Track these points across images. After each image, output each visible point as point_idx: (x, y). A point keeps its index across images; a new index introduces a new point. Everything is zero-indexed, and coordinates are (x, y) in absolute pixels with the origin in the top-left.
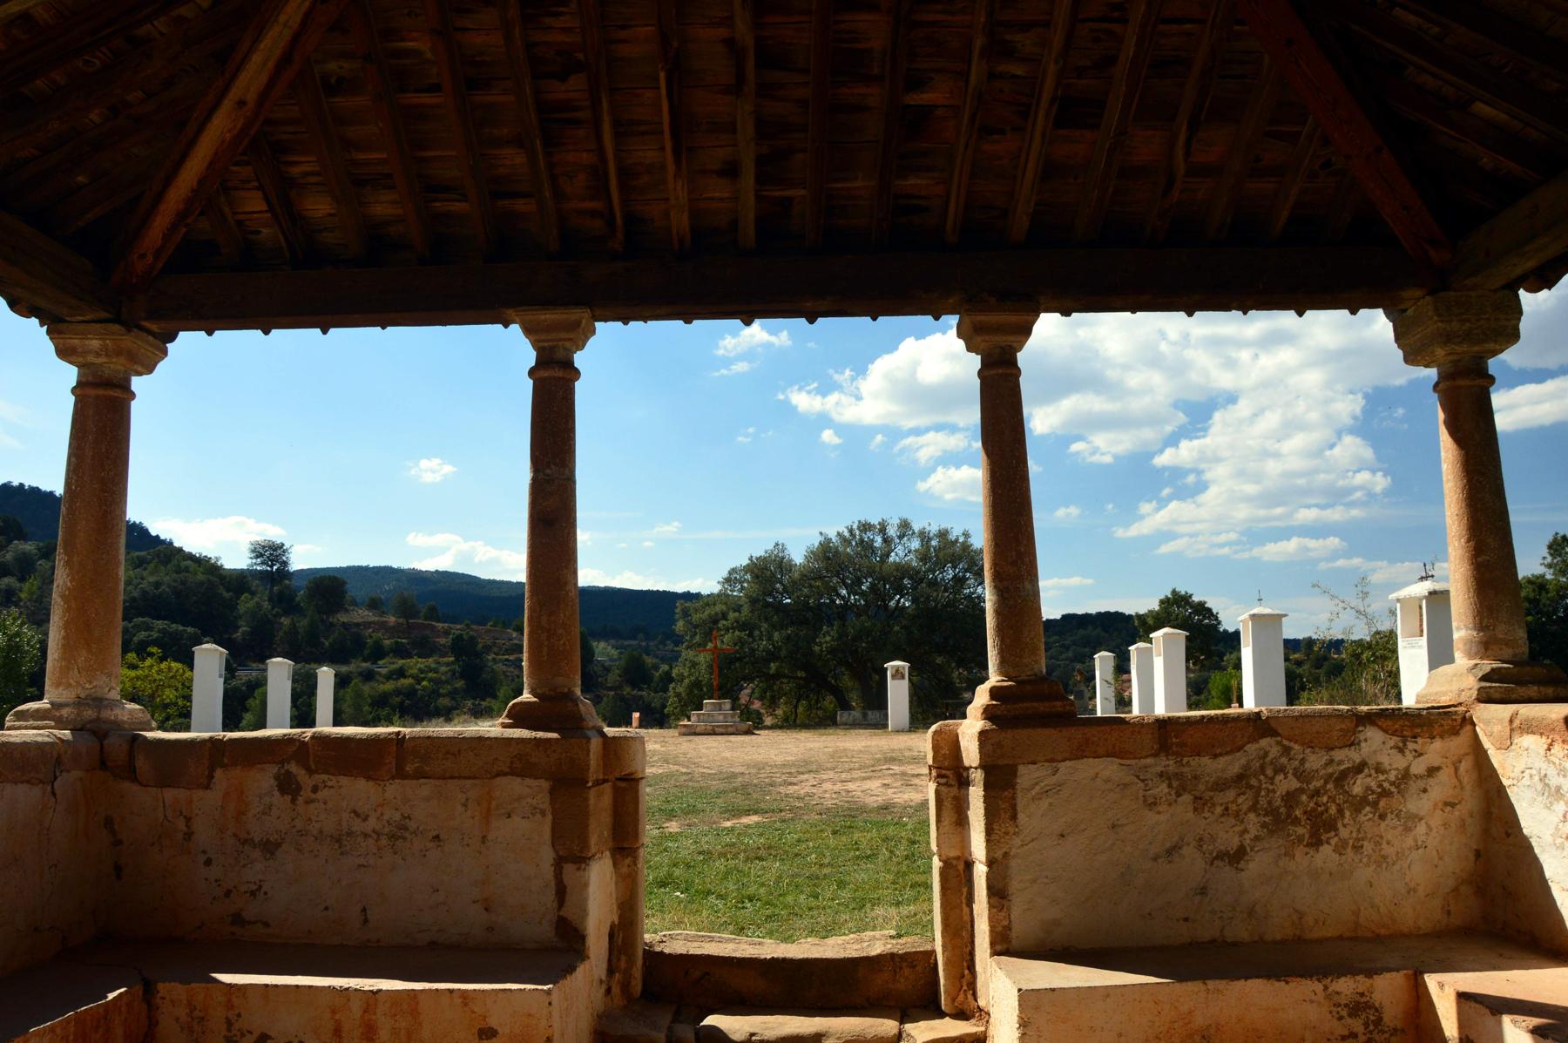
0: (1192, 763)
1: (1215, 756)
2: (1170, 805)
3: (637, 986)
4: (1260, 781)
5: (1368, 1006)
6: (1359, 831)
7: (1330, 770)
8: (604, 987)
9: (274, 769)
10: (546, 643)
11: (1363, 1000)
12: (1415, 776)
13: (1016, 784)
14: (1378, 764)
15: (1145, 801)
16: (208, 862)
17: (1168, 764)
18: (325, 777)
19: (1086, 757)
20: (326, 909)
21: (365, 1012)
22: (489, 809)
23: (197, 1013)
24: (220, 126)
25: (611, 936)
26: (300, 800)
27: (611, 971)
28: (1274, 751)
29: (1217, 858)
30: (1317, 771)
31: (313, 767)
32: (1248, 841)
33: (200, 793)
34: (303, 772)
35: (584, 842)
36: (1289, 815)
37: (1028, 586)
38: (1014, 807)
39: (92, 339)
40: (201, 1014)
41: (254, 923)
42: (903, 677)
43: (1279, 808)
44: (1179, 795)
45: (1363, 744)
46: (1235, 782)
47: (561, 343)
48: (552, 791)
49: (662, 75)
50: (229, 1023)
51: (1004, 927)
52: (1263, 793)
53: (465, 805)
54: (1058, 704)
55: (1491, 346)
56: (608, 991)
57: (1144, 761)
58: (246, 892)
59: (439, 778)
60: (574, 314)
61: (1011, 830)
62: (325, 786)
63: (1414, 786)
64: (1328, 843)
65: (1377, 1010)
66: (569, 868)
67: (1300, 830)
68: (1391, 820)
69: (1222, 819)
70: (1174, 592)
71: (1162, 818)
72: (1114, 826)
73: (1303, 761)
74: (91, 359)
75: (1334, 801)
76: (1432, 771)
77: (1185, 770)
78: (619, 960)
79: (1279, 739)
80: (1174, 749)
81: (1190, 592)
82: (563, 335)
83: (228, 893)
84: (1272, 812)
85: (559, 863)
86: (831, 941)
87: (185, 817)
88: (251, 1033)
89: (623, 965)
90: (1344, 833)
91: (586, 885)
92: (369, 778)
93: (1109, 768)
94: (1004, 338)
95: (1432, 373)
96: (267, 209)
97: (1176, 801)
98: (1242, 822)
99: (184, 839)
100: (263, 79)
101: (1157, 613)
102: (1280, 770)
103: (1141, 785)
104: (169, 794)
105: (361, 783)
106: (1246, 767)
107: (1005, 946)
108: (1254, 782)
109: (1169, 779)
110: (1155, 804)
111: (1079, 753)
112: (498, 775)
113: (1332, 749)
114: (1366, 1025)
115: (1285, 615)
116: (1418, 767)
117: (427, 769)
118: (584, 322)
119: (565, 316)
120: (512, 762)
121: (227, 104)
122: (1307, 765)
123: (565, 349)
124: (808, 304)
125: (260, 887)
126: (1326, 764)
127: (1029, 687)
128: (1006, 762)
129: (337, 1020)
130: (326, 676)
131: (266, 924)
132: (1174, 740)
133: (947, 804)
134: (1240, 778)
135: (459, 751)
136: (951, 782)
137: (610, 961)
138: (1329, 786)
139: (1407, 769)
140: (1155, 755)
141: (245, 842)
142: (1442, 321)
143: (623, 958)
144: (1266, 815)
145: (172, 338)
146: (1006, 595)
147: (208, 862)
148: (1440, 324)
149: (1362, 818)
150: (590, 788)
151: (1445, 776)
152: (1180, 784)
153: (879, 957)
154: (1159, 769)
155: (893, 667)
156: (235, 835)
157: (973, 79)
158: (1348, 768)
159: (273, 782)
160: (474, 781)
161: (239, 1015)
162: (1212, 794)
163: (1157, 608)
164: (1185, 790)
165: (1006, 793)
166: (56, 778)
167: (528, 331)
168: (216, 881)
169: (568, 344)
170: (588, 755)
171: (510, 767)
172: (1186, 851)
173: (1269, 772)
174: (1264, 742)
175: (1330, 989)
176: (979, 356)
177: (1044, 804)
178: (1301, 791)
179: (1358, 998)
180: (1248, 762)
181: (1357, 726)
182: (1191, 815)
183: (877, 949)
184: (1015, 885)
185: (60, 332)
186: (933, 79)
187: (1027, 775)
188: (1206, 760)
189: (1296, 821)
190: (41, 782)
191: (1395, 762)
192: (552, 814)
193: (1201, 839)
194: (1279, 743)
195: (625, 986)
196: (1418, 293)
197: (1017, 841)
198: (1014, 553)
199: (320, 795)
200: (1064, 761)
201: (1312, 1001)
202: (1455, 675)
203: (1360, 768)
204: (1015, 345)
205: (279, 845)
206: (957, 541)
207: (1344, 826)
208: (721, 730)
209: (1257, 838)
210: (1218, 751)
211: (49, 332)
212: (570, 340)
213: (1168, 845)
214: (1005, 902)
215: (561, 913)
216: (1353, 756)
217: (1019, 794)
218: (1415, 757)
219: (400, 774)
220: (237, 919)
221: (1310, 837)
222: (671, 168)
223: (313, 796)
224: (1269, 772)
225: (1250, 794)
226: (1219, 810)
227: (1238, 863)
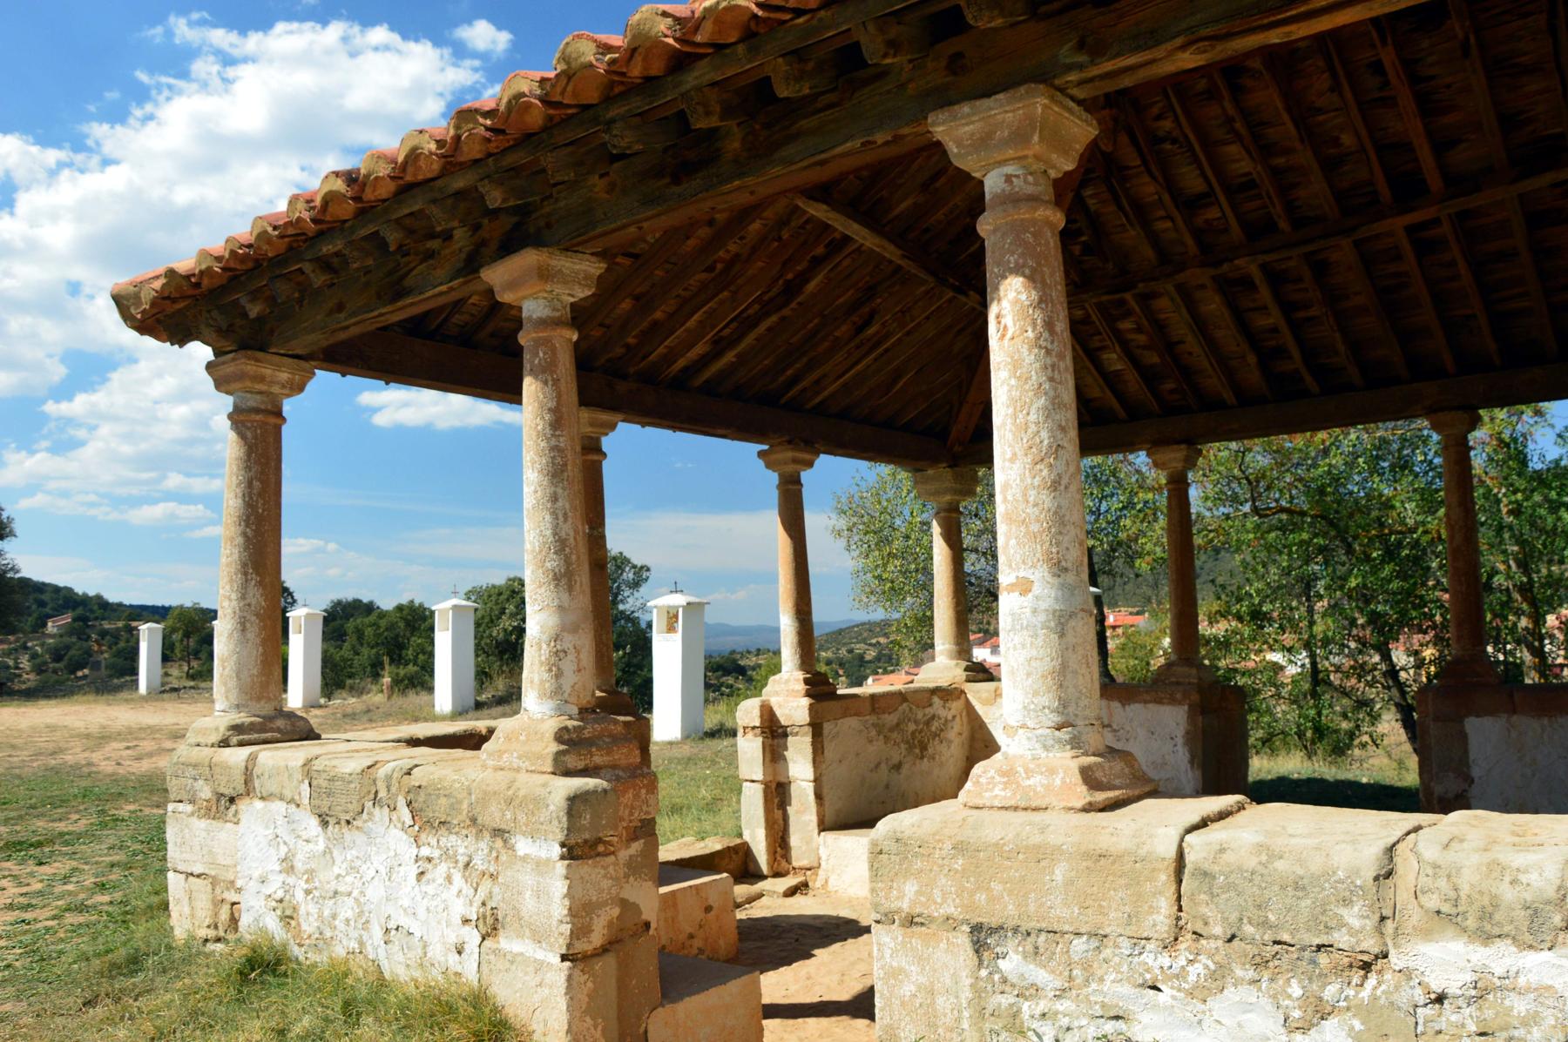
17: (872, 719)
63: (950, 725)
68: (944, 744)
76: (954, 717)
84: (907, 742)
93: (852, 723)
133: (767, 749)
134: (898, 725)
151: (958, 719)
174: (905, 705)
183: (718, 847)
184: (825, 791)
187: (828, 727)
191: (943, 713)
203: (933, 717)
216: (930, 711)
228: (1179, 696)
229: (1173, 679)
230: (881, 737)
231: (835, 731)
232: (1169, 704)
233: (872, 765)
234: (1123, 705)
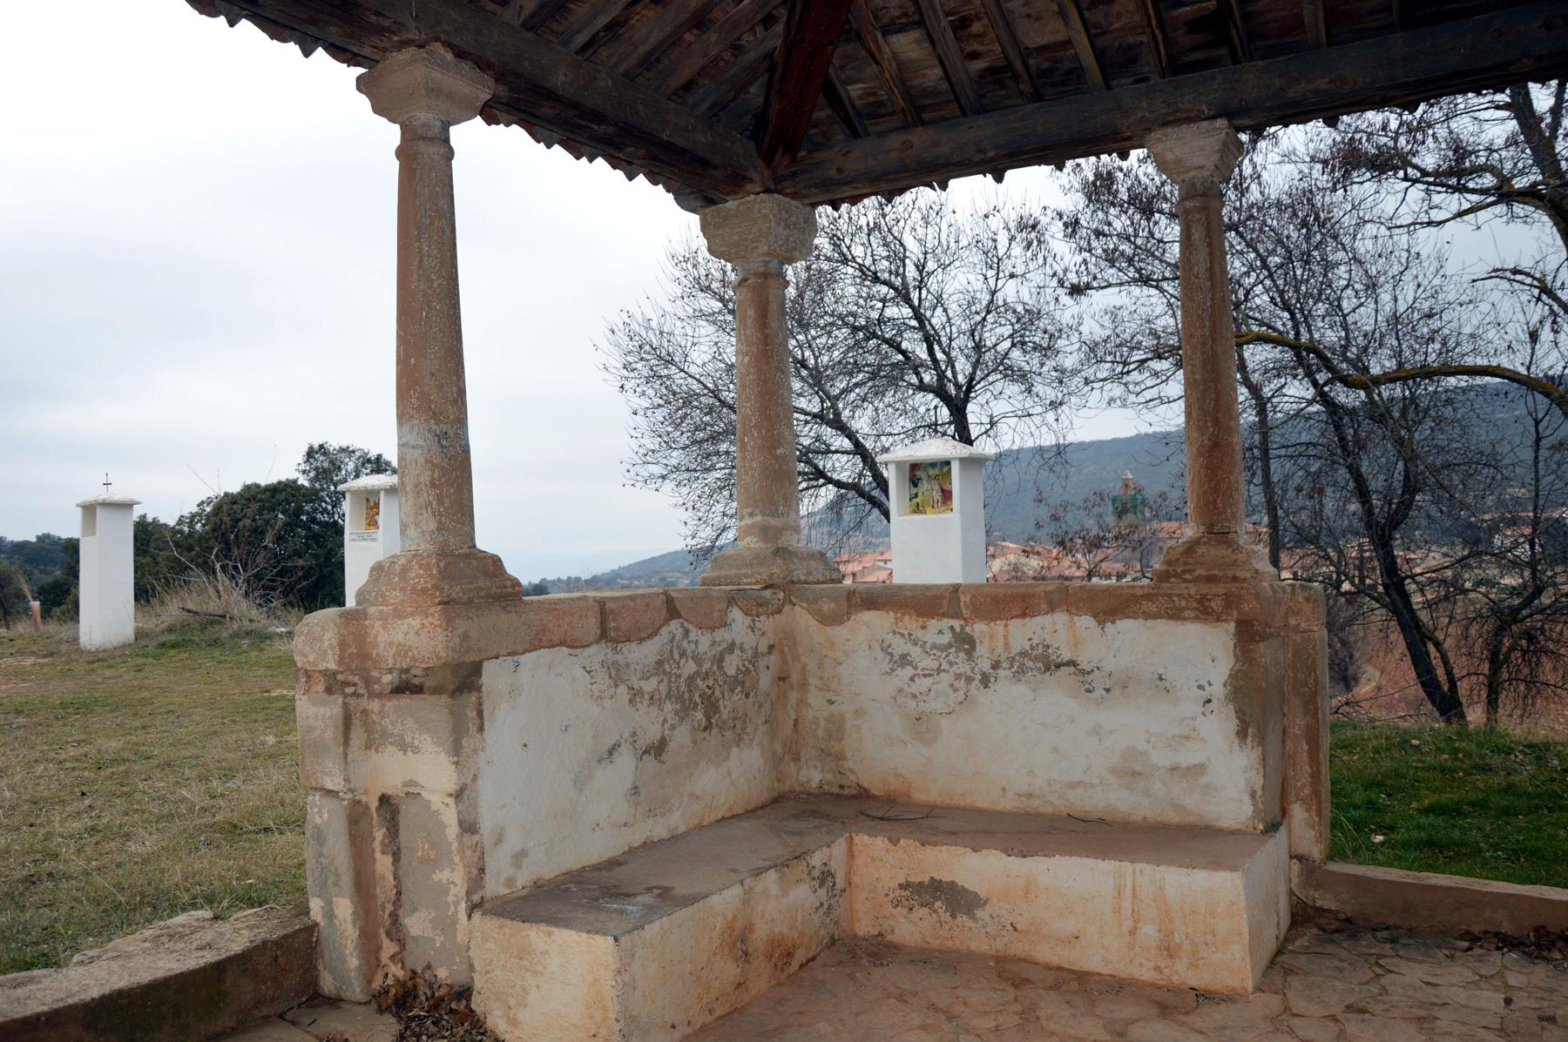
1: (641, 640)
28: (679, 633)
29: (645, 752)
38: (480, 714)
44: (616, 686)
77: (619, 657)
84: (679, 698)
108: (667, 667)
122: (700, 647)
134: (660, 663)
136: (361, 691)
140: (598, 641)
146: (444, 442)
149: (735, 698)
172: (625, 748)
174: (675, 625)
178: (697, 673)
188: (634, 646)
200: (524, 653)
202: (756, 558)
203: (731, 648)
210: (643, 635)
224: (676, 656)
228: (1216, 604)
229: (1200, 572)
230: (622, 689)
232: (1196, 619)
234: (1101, 623)
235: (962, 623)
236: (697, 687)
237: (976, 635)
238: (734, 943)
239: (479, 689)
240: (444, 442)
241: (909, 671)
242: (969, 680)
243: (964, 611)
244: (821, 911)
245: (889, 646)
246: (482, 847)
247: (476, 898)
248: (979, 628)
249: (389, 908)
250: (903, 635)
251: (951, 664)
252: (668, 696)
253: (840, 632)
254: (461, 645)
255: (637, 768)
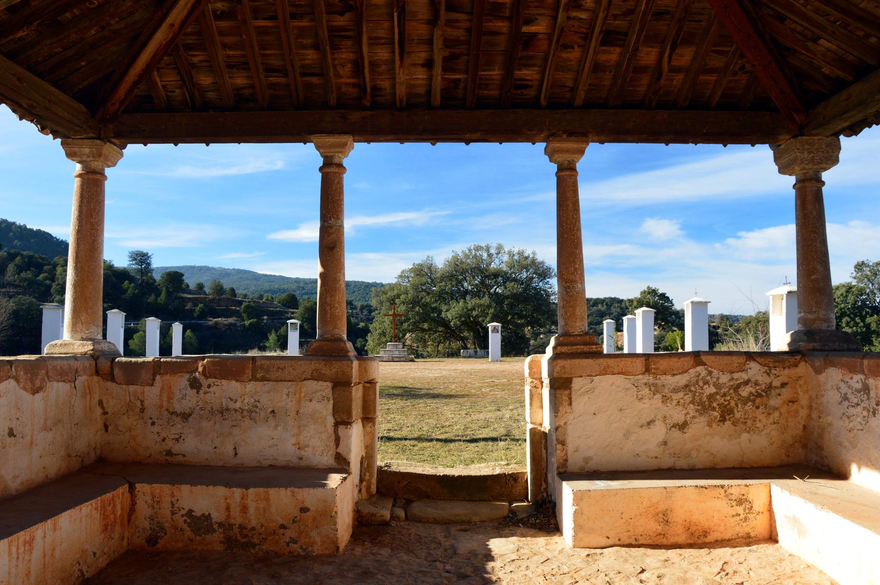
0: (662, 378)
1: (674, 375)
2: (650, 399)
3: (374, 489)
4: (696, 388)
5: (746, 500)
6: (745, 414)
7: (731, 383)
8: (358, 488)
9: (187, 376)
10: (329, 311)
11: (744, 497)
12: (775, 387)
13: (571, 388)
14: (757, 380)
15: (637, 397)
16: (153, 424)
18: (214, 380)
19: (608, 374)
20: (215, 448)
21: (242, 499)
22: (300, 398)
23: (156, 499)
24: (160, 36)
25: (361, 463)
26: (201, 392)
27: (361, 481)
29: (673, 427)
30: (725, 384)
31: (208, 375)
32: (689, 419)
33: (147, 389)
34: (203, 377)
35: (349, 414)
36: (710, 406)
37: (580, 286)
38: (570, 399)
39: (85, 148)
40: (159, 500)
41: (178, 455)
42: (498, 332)
43: (705, 402)
44: (654, 394)
45: (749, 370)
46: (683, 388)
47: (336, 154)
48: (333, 388)
49: (395, 14)
50: (173, 505)
51: (564, 460)
52: (697, 394)
53: (288, 395)
54: (594, 347)
55: (824, 166)
56: (360, 491)
57: (637, 377)
58: (173, 439)
59: (274, 381)
60: (344, 138)
61: (569, 411)
62: (214, 385)
63: (774, 392)
64: (729, 420)
65: (750, 502)
66: (341, 430)
67: (716, 414)
69: (676, 407)
70: (648, 287)
71: (646, 406)
72: (621, 410)
73: (718, 378)
74: (84, 158)
75: (733, 400)
77: (658, 382)
78: (365, 475)
79: (706, 367)
80: (653, 371)
81: (657, 288)
82: (337, 150)
83: (164, 440)
84: (701, 404)
85: (337, 425)
86: (473, 466)
87: (141, 400)
88: (184, 509)
89: (367, 477)
90: (738, 415)
91: (350, 436)
92: (237, 381)
93: (620, 379)
94: (570, 156)
95: (792, 180)
96: (180, 79)
97: (653, 398)
98: (686, 409)
99: (140, 412)
100: (185, 12)
101: (640, 299)
102: (706, 383)
103: (635, 389)
104: (132, 388)
105: (234, 383)
106: (689, 381)
107: (564, 469)
108: (693, 389)
109: (650, 386)
110: (642, 399)
111: (604, 372)
112: (305, 379)
113: (733, 373)
114: (745, 510)
115: (709, 302)
116: (776, 383)
117: (267, 376)
118: (349, 143)
119: (339, 140)
120: (312, 373)
121: (165, 26)
122: (720, 381)
123: (339, 157)
124: (467, 136)
125: (181, 436)
126: (730, 380)
127: (579, 338)
128: (566, 376)
129: (227, 503)
130: (177, 329)
131: (184, 456)
132: (653, 366)
134: (686, 386)
135: (285, 367)
137: (361, 475)
138: (731, 391)
139: (771, 383)
140: (643, 374)
141: (172, 413)
142: (799, 152)
143: (367, 474)
144: (698, 406)
145: (125, 147)
147: (153, 424)
148: (798, 154)
149: (747, 408)
150: (353, 387)
152: (655, 389)
153: (499, 476)
154: (645, 381)
155: (492, 326)
156: (167, 410)
157: (559, 20)
158: (741, 383)
159: (187, 383)
160: (292, 383)
161: (178, 500)
162: (671, 394)
163: (639, 296)
164: (657, 392)
165: (566, 392)
166: (76, 380)
167: (318, 148)
168: (158, 433)
169: (340, 155)
170: (352, 369)
171: (312, 376)
172: (657, 422)
173: (701, 384)
174: (699, 369)
175: (728, 492)
176: (556, 165)
177: (586, 398)
178: (717, 393)
179: (741, 496)
180: (690, 378)
181: (746, 361)
182: (660, 404)
183: (497, 471)
185: (68, 144)
186: (537, 19)
188: (668, 377)
189: (714, 409)
190: (70, 381)
192: (333, 400)
193: (665, 417)
194: (706, 369)
195: (368, 488)
196: (787, 137)
197: (571, 416)
198: (573, 269)
199: (211, 389)
200: (596, 376)
201: (718, 498)
203: (747, 383)
204: (575, 160)
205: (190, 415)
206: (529, 256)
207: (738, 412)
208: (398, 360)
209: (694, 417)
210: (675, 373)
211: (62, 144)
212: (341, 152)
213: (648, 420)
214: (564, 447)
215: (338, 451)
217: (573, 393)
218: (775, 378)
219: (254, 379)
220: (169, 453)
221: (720, 417)
222: (398, 63)
223: (208, 390)
224: (701, 384)
225: (690, 395)
226: (675, 402)
227: (683, 429)
231: (590, 386)
233: (644, 421)
235: (865, 377)
236: (715, 400)
237: (870, 385)
238: (657, 514)
239: (570, 389)
240: (568, 290)
241: (846, 403)
242: (868, 411)
243: (866, 370)
244: (738, 518)
245: (840, 388)
246: (566, 451)
247: (562, 470)
248: (871, 381)
249: (545, 471)
250: (844, 382)
251: (862, 401)
252: (692, 402)
253: (822, 377)
254: (561, 371)
255: (667, 433)
